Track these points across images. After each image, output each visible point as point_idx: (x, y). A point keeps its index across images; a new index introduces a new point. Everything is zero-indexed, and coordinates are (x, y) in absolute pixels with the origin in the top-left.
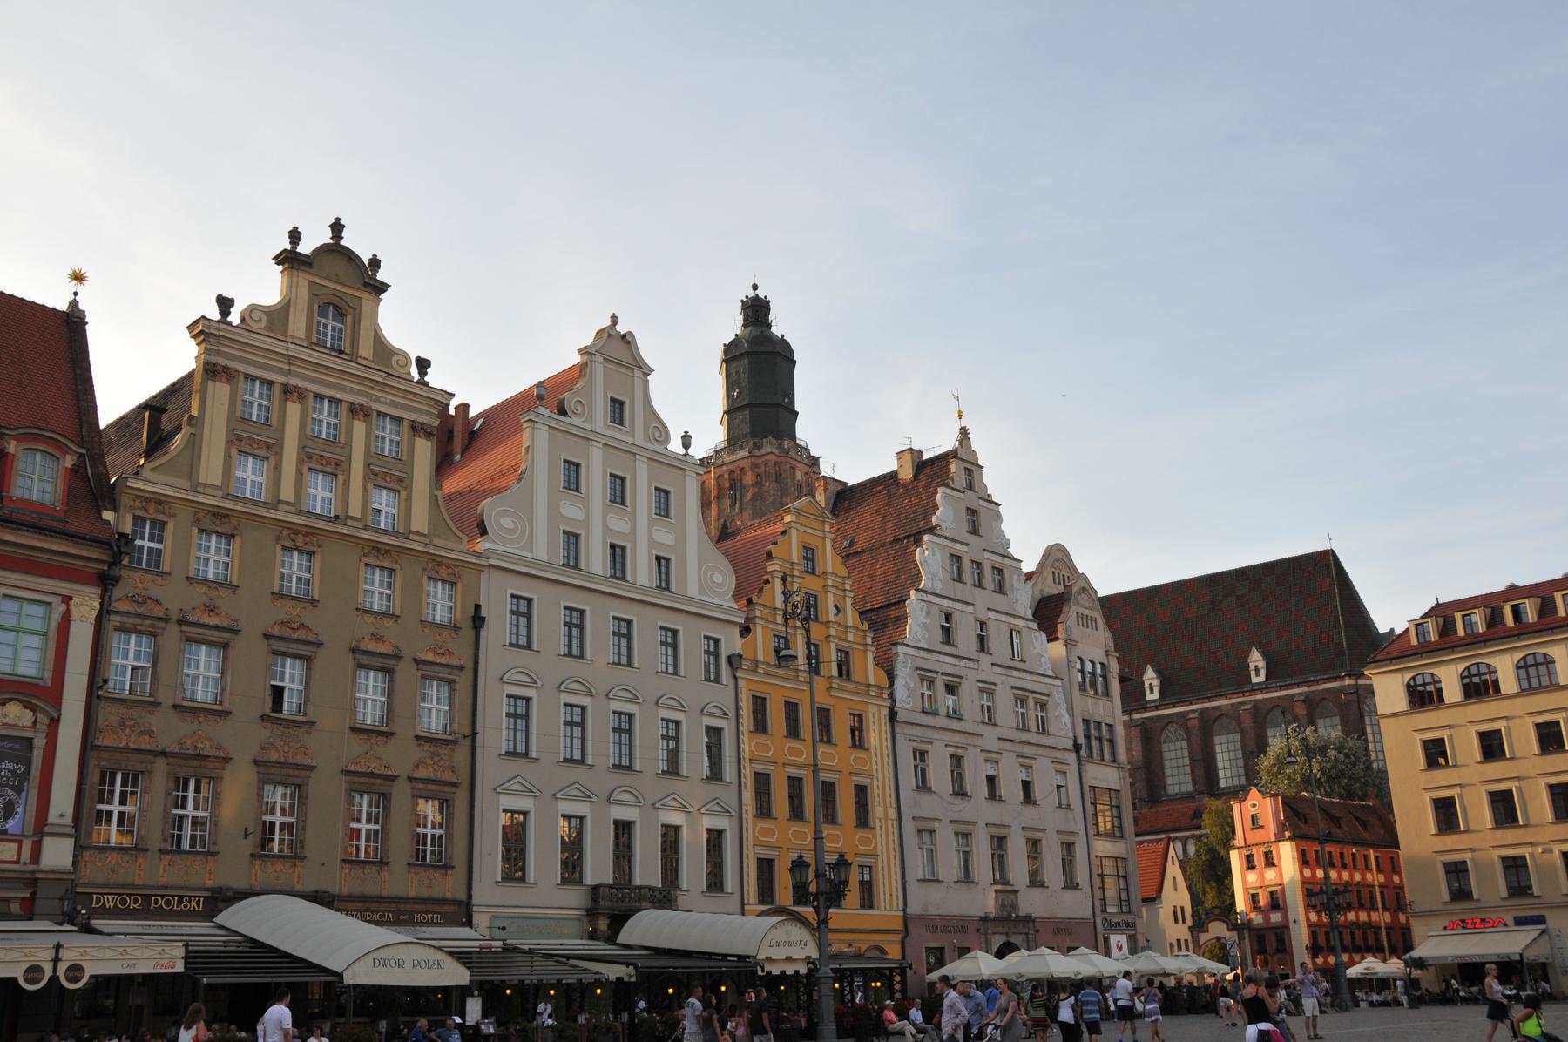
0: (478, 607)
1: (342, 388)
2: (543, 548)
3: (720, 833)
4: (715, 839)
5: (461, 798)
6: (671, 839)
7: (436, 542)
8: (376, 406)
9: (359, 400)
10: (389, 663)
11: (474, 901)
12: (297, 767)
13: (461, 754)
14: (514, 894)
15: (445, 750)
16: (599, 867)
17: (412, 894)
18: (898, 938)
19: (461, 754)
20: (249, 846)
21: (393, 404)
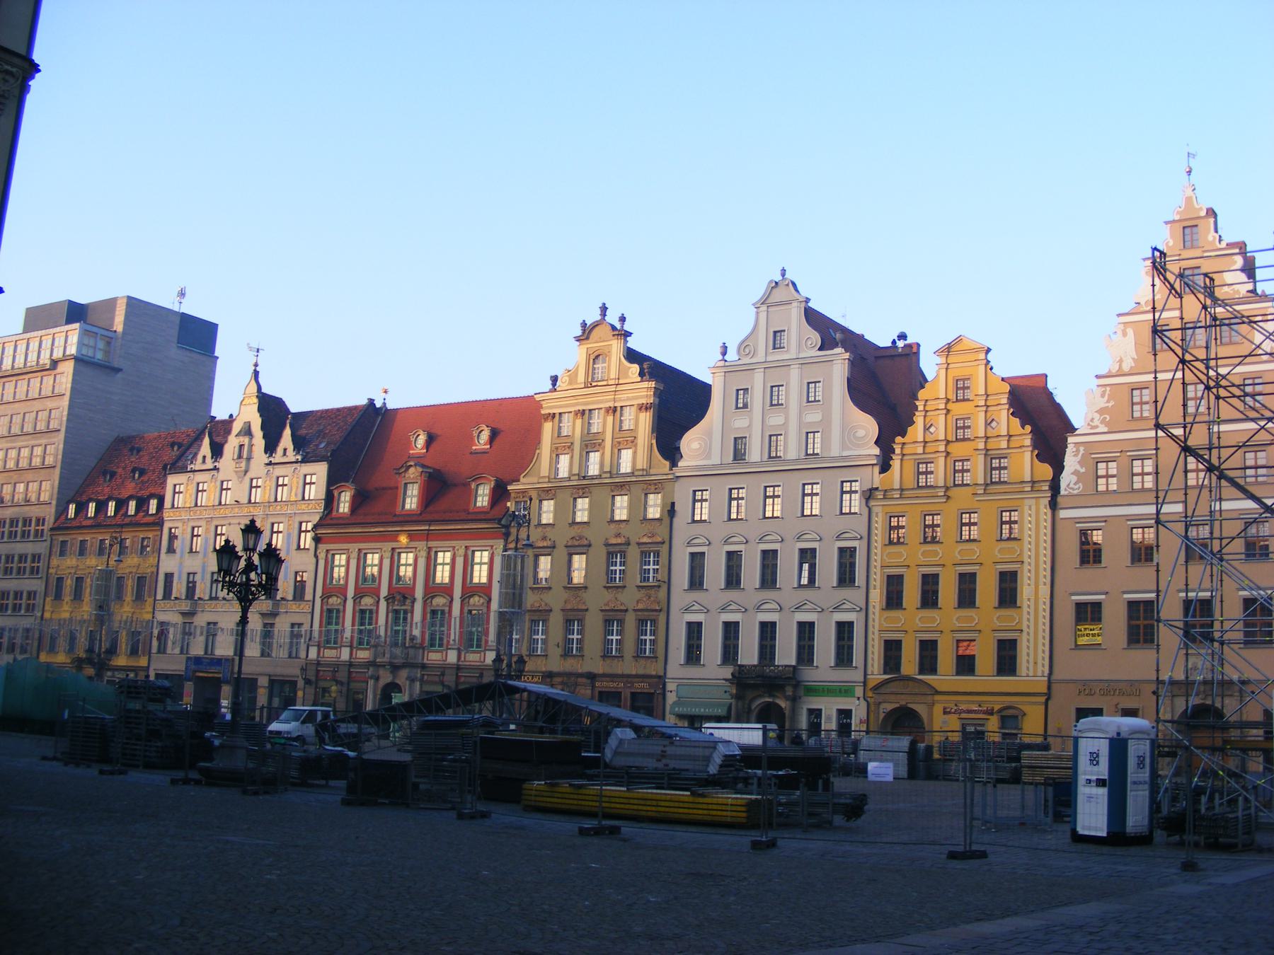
0: (673, 504)
1: (601, 402)
2: (718, 455)
3: (851, 624)
4: (844, 630)
5: (662, 618)
6: (806, 630)
7: (652, 471)
8: (618, 404)
9: (608, 405)
10: (623, 548)
11: (669, 675)
12: (578, 610)
13: (662, 593)
14: (693, 672)
15: (652, 592)
16: (749, 654)
17: (634, 673)
18: (1043, 699)
19: (662, 593)
20: (559, 651)
21: (628, 399)
